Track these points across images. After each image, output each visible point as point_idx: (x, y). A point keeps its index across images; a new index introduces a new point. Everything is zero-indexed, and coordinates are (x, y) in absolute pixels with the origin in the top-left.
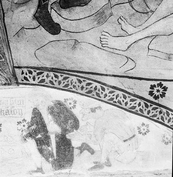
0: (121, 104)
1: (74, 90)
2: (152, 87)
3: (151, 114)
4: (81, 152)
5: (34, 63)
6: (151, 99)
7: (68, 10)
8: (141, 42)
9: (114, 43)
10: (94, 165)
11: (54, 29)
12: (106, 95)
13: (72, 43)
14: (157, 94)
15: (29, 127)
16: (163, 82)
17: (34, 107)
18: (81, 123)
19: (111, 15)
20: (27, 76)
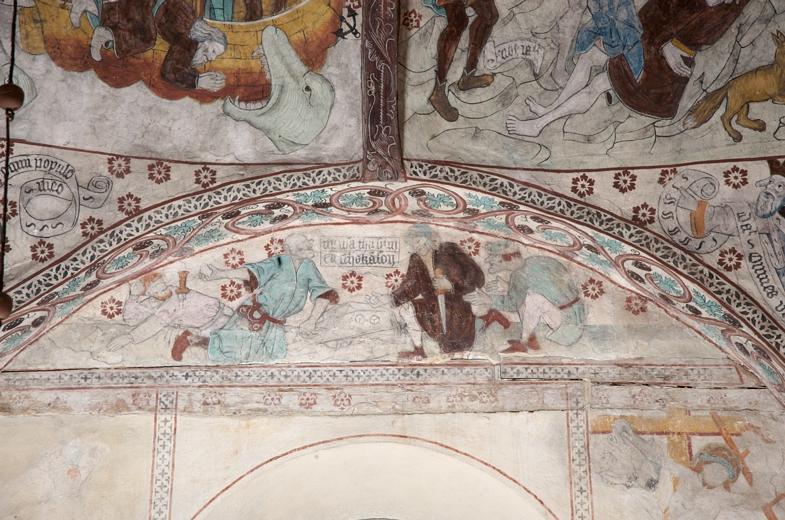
0: (534, 203)
1: (474, 186)
2: (575, 181)
3: (575, 216)
4: (488, 325)
5: (426, 155)
6: (576, 196)
7: (467, 92)
8: (553, 126)
9: (524, 128)
10: (509, 346)
11: (451, 114)
12: (515, 193)
13: (472, 131)
14: (582, 190)
15: (404, 282)
16: (587, 174)
17: (412, 252)
18: (489, 278)
19: (517, 96)
20: (417, 171)
